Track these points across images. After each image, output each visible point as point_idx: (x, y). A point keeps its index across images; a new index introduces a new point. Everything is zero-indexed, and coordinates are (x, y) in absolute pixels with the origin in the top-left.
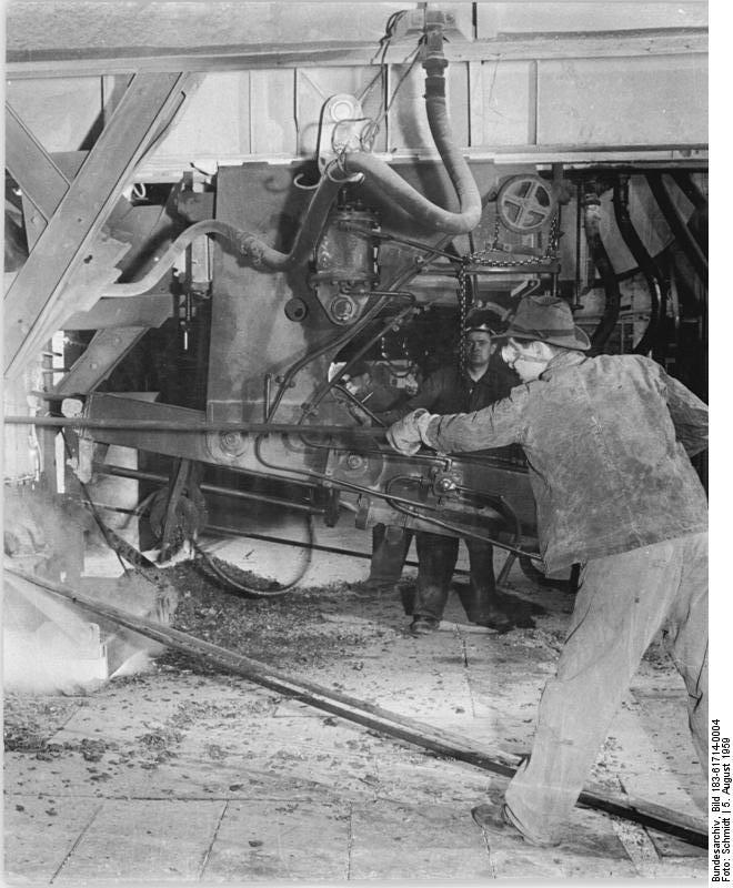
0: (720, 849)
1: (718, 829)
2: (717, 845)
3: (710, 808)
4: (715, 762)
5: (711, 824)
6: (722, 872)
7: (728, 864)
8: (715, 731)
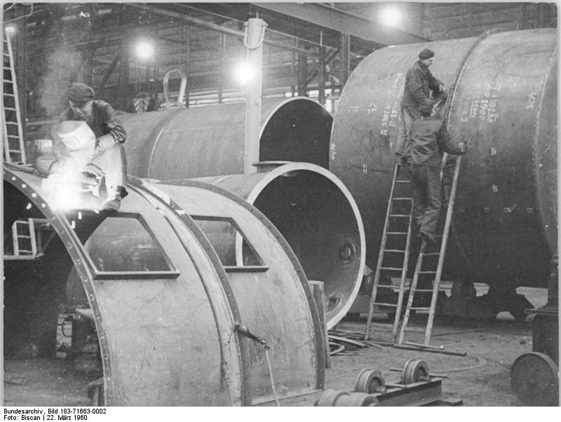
0: (24, 414)
1: (38, 412)
2: (27, 412)
3: (49, 408)
5: (41, 408)
6: (10, 415)
8: (96, 411)
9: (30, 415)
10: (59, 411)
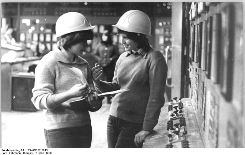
1: (16, 151)
4: (46, 150)
6: (4, 152)
7: (6, 153)
10: (26, 150)
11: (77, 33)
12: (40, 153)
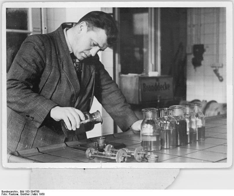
1: (16, 192)
2: (11, 192)
6: (4, 193)
9: (13, 193)
10: (25, 191)
11: (86, 115)
12: (34, 194)
